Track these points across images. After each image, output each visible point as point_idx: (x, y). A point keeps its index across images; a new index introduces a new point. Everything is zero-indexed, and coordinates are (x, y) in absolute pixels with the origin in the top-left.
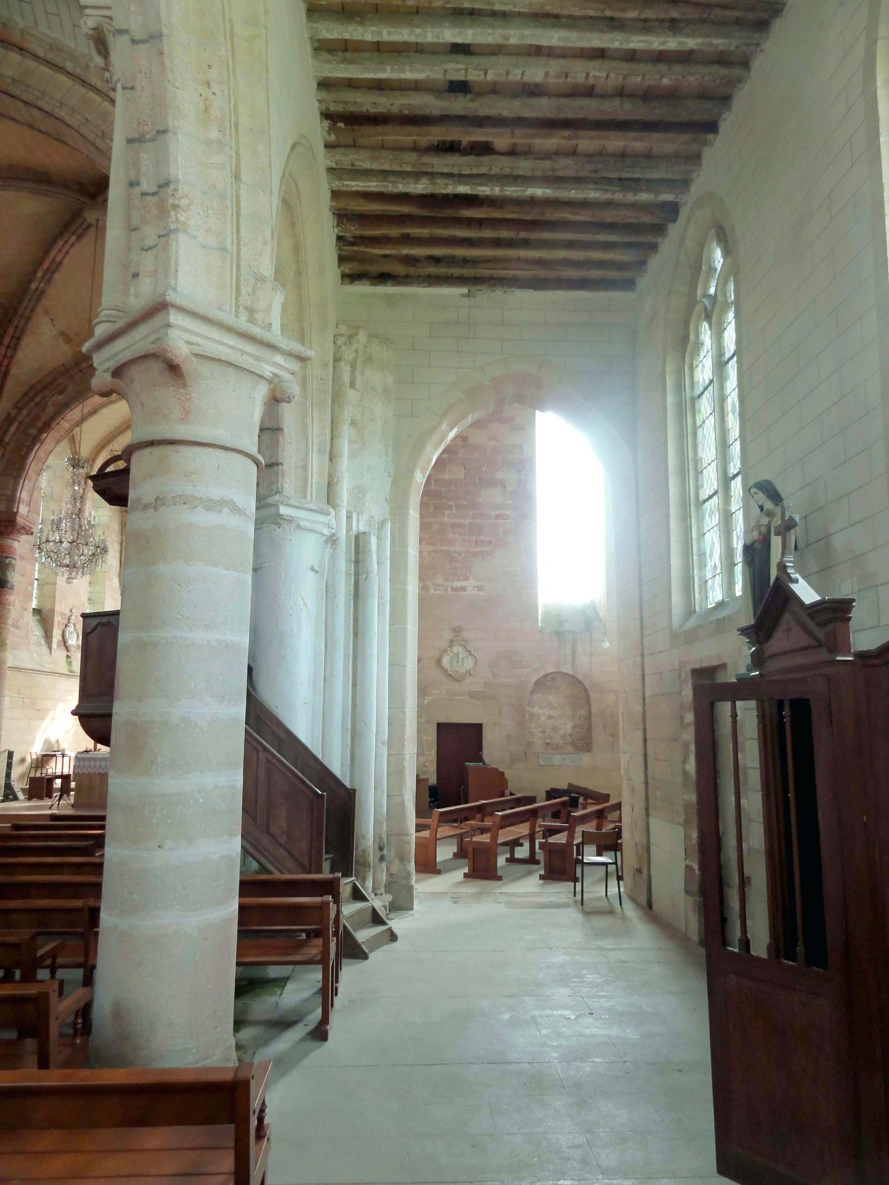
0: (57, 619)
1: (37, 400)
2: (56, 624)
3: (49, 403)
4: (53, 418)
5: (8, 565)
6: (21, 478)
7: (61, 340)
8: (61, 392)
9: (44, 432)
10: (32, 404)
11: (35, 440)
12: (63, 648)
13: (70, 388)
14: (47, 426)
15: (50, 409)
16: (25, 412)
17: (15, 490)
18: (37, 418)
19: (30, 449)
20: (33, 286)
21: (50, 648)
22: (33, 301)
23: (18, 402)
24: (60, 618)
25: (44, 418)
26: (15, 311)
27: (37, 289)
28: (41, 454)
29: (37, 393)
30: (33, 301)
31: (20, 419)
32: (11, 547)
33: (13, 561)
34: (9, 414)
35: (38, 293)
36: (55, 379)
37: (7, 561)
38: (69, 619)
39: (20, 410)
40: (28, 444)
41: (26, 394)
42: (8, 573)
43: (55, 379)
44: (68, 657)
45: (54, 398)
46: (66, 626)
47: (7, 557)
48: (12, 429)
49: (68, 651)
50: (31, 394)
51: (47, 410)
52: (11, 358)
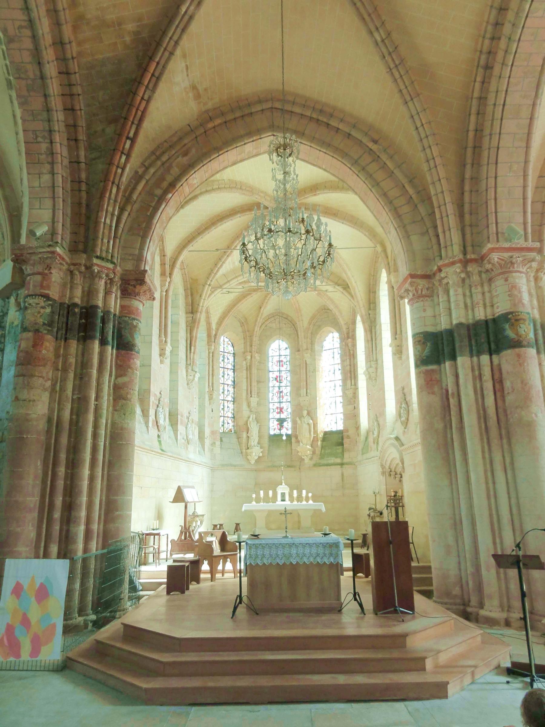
0: (152, 399)
1: (165, 158)
2: (151, 404)
3: (174, 164)
4: (178, 179)
5: (136, 327)
6: (147, 238)
7: (191, 95)
8: (185, 154)
9: (170, 192)
10: (159, 163)
11: (161, 199)
12: (156, 427)
13: (193, 151)
14: (172, 186)
15: (175, 171)
16: (152, 171)
17: (142, 249)
18: (162, 179)
19: (156, 209)
20: (183, 9)
21: (147, 427)
22: (179, 31)
23: (145, 161)
24: (153, 398)
25: (169, 178)
26: (159, 44)
27: (186, 12)
28: (164, 216)
29: (164, 153)
30: (179, 31)
31: (147, 177)
32: (137, 309)
33: (140, 324)
34: (137, 172)
35: (187, 18)
36: (181, 139)
37: (135, 323)
38: (159, 400)
39: (147, 169)
40: (153, 204)
41: (153, 153)
42: (135, 336)
43: (181, 139)
44: (159, 436)
45: (180, 159)
46: (158, 406)
47: (134, 319)
48: (140, 187)
49: (159, 431)
50: (158, 153)
51: (171, 172)
52: (148, 101)
